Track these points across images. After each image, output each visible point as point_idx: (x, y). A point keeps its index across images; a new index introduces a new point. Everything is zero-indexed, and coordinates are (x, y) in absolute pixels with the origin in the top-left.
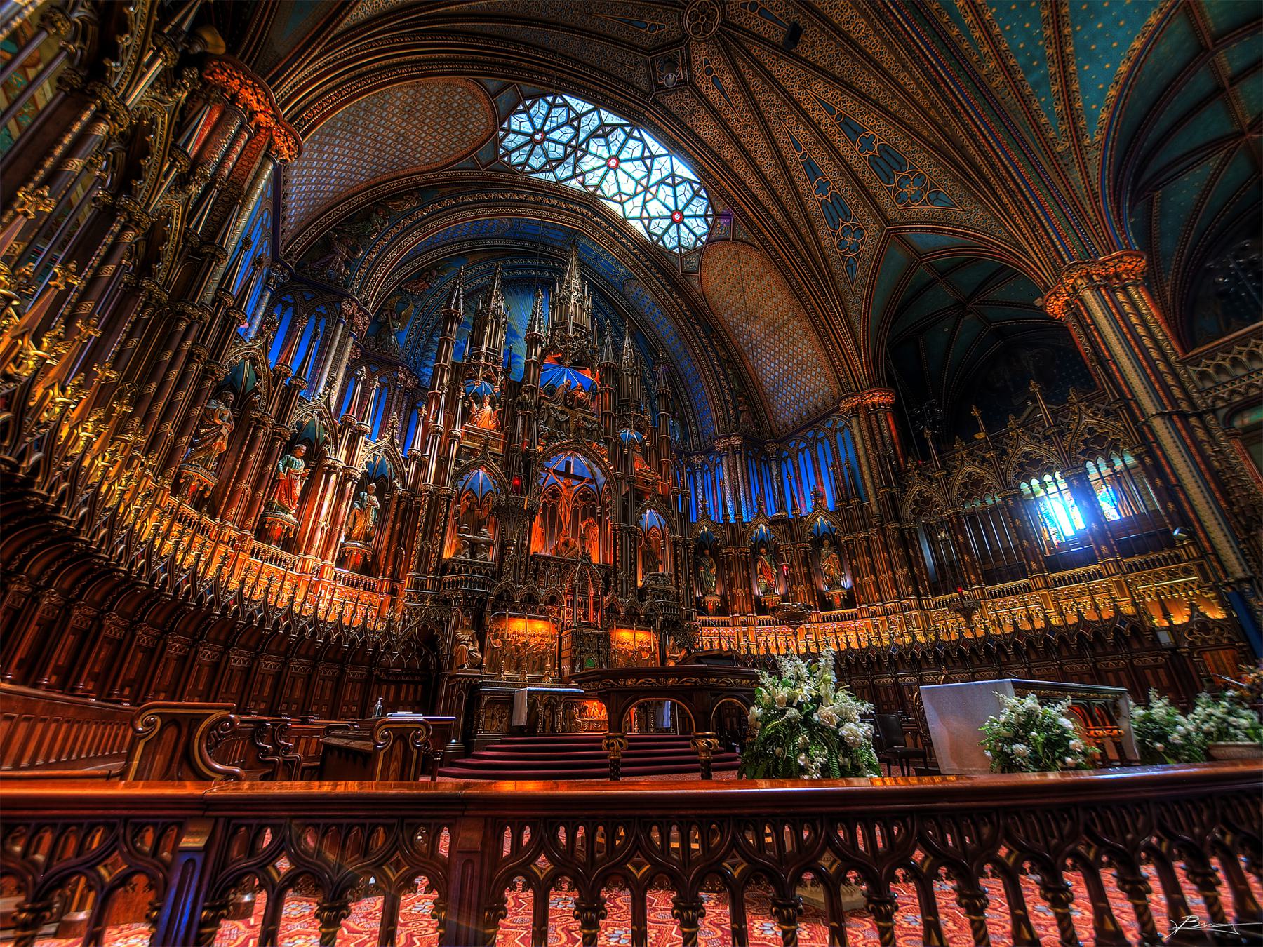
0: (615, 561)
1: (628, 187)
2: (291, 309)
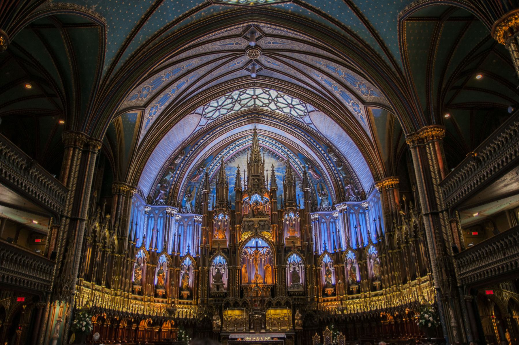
1: (266, 101)
2: (153, 219)
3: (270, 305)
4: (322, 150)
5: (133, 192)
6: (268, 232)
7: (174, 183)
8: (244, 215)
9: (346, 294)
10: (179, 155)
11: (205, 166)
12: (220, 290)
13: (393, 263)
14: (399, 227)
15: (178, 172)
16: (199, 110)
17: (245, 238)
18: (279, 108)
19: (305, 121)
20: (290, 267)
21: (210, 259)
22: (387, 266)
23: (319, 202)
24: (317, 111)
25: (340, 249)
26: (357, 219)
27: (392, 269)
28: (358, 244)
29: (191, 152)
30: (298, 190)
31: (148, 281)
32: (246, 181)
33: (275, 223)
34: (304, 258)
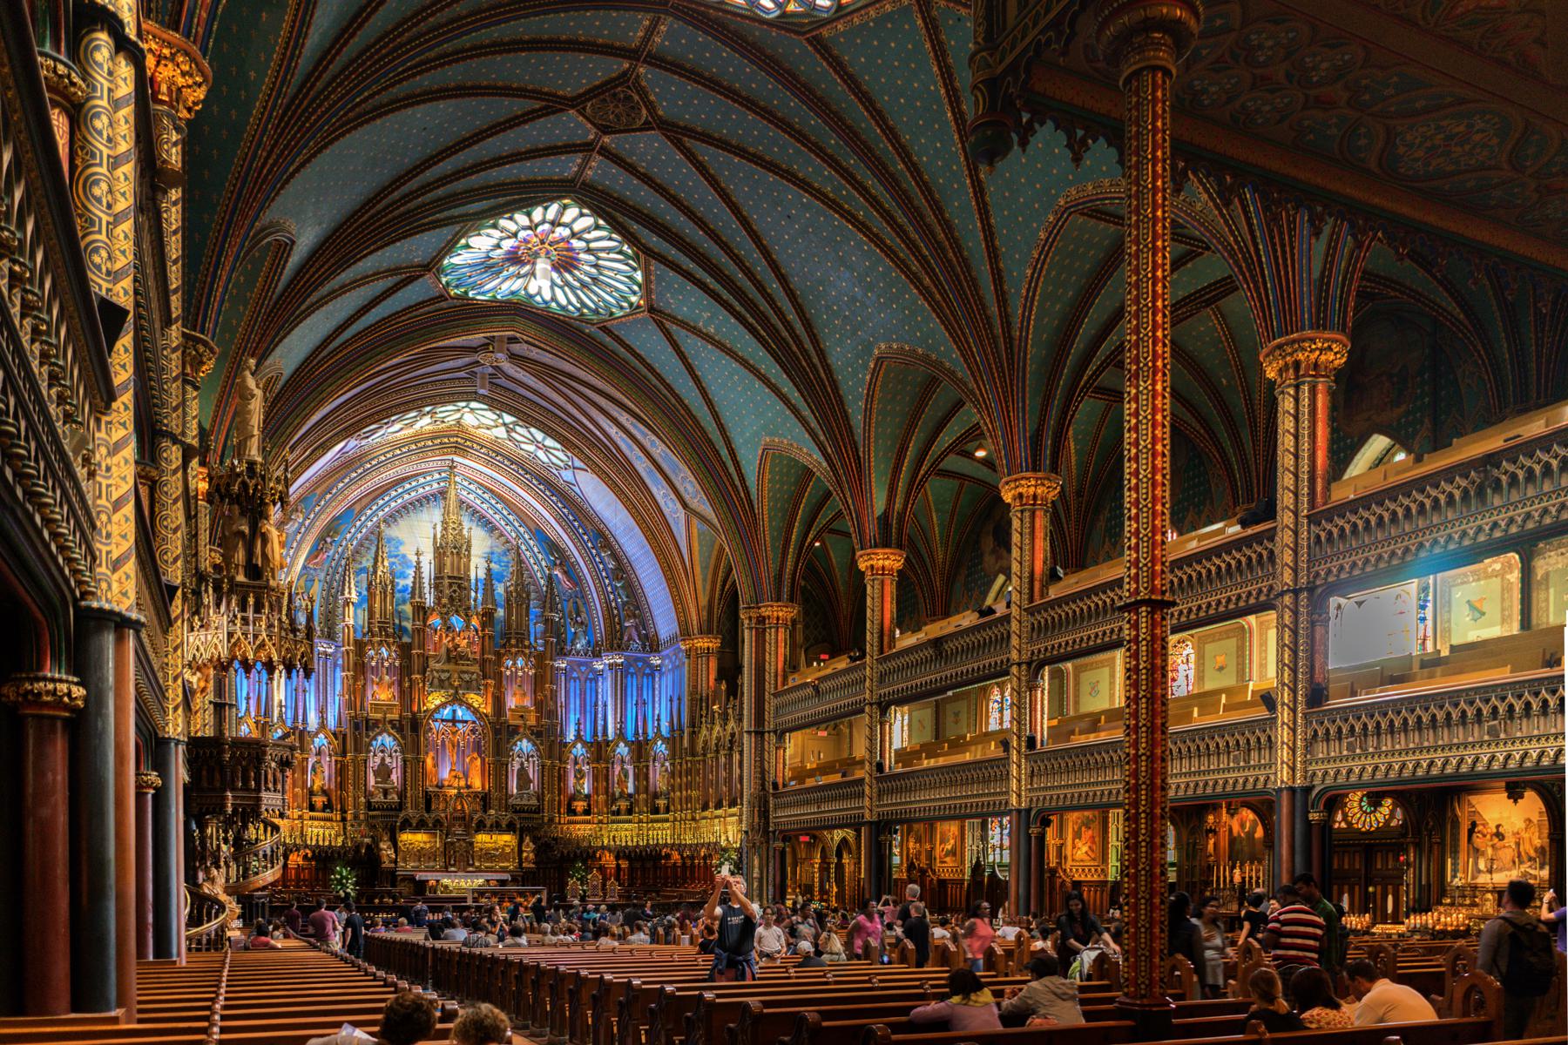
3: (481, 827)
4: (589, 540)
23: (569, 637)
27: (689, 786)
30: (535, 610)
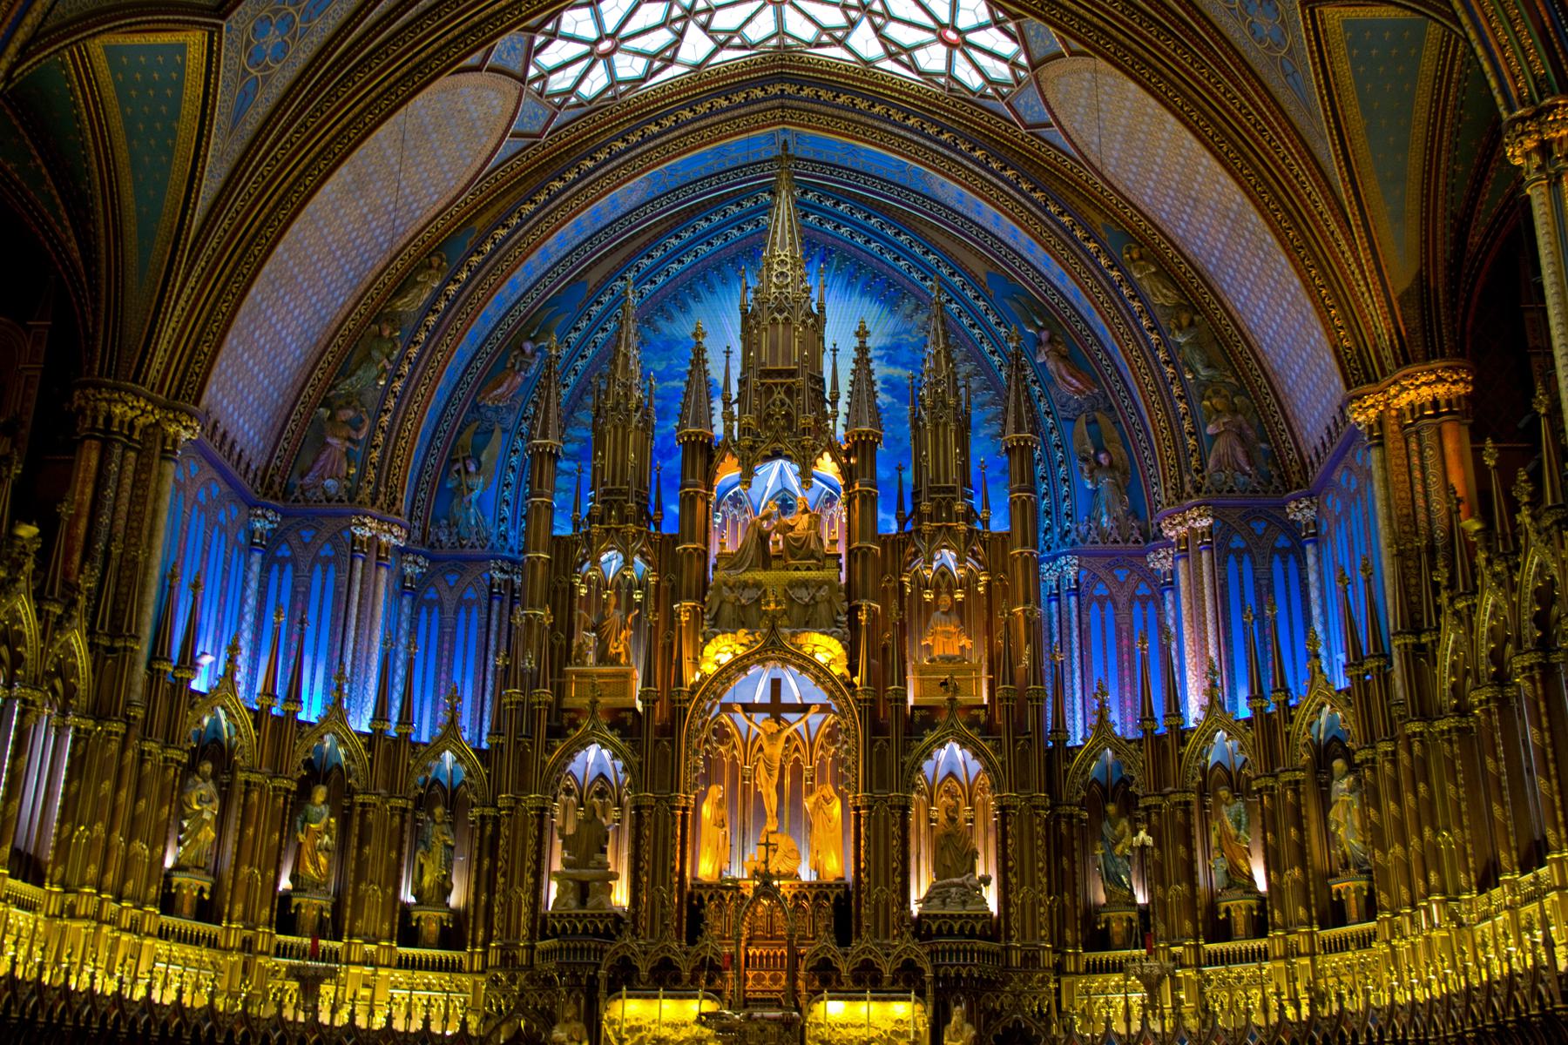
0: (858, 870)
2: (289, 568)
3: (828, 981)
4: (1103, 248)
5: (177, 433)
6: (830, 635)
7: (391, 403)
8: (720, 557)
9: (1197, 939)
10: (418, 271)
11: (545, 331)
12: (591, 902)
13: (1428, 783)
14: (1460, 605)
15: (414, 352)
16: (506, 47)
17: (717, 663)
18: (894, 51)
19: (1021, 111)
20: (931, 802)
21: (550, 760)
22: (1399, 800)
24: (1072, 54)
25: (1174, 721)
26: (1264, 582)
28: (1261, 696)
29: (476, 259)
31: (246, 855)
32: (735, 396)
33: (865, 596)
34: (996, 760)
